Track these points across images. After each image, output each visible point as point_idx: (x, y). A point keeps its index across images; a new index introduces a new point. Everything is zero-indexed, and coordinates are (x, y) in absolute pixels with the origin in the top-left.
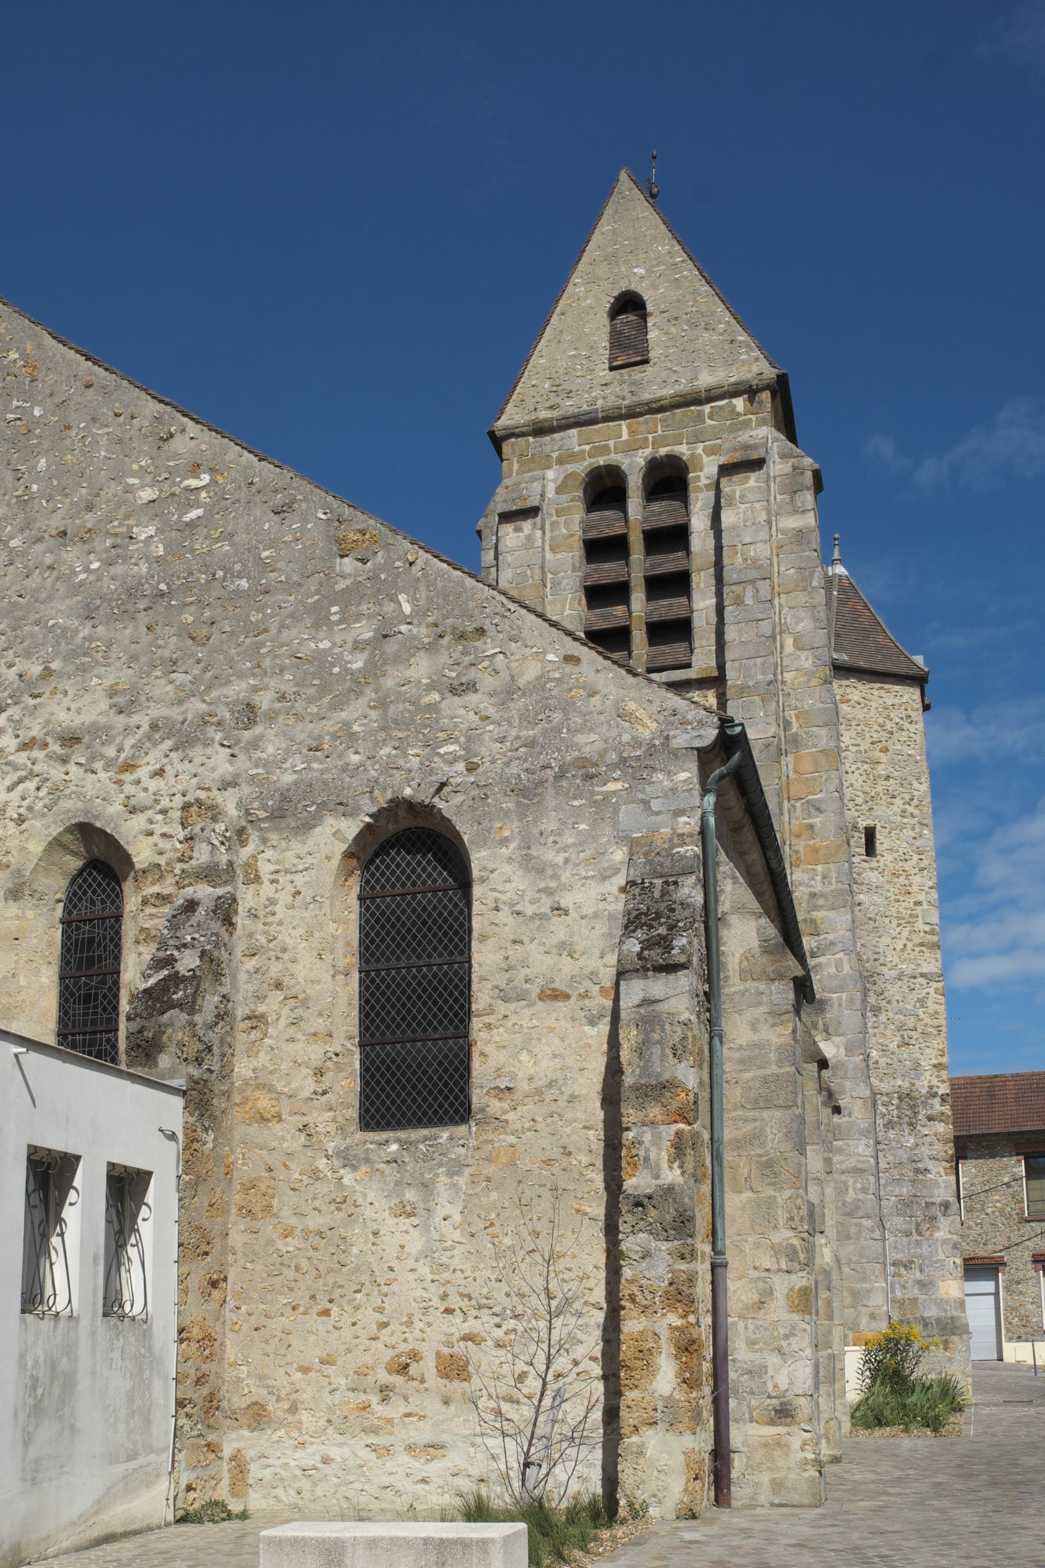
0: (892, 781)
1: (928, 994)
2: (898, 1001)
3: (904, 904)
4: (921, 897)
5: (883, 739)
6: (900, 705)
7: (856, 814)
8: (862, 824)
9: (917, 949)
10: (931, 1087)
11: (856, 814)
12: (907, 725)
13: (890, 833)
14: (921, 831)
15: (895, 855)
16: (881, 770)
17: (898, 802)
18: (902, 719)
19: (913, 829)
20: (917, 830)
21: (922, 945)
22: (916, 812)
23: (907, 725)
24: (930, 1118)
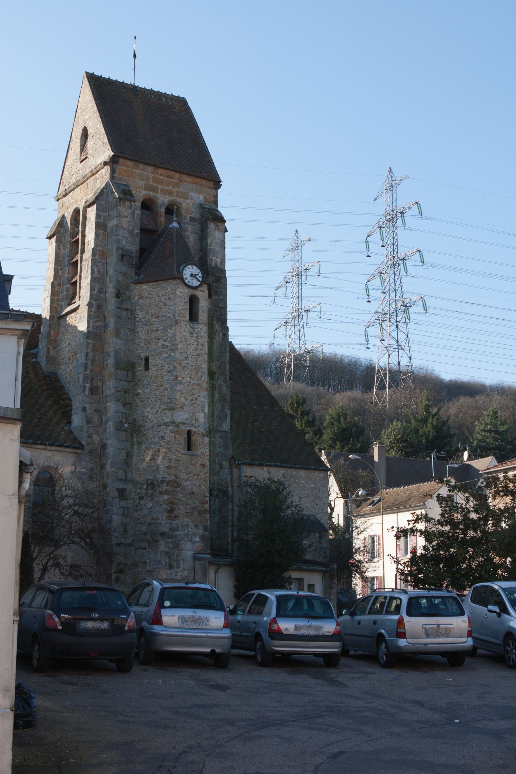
0: (159, 332)
1: (166, 433)
2: (151, 438)
3: (159, 391)
4: (168, 386)
5: (157, 312)
6: (166, 293)
7: (141, 351)
8: (143, 355)
9: (163, 412)
10: (163, 478)
11: (141, 351)
12: (168, 302)
13: (155, 357)
14: (171, 354)
15: (157, 368)
16: (154, 327)
17: (161, 341)
18: (166, 300)
19: (167, 353)
20: (169, 353)
21: (165, 409)
22: (169, 345)
23: (168, 302)
24: (161, 493)
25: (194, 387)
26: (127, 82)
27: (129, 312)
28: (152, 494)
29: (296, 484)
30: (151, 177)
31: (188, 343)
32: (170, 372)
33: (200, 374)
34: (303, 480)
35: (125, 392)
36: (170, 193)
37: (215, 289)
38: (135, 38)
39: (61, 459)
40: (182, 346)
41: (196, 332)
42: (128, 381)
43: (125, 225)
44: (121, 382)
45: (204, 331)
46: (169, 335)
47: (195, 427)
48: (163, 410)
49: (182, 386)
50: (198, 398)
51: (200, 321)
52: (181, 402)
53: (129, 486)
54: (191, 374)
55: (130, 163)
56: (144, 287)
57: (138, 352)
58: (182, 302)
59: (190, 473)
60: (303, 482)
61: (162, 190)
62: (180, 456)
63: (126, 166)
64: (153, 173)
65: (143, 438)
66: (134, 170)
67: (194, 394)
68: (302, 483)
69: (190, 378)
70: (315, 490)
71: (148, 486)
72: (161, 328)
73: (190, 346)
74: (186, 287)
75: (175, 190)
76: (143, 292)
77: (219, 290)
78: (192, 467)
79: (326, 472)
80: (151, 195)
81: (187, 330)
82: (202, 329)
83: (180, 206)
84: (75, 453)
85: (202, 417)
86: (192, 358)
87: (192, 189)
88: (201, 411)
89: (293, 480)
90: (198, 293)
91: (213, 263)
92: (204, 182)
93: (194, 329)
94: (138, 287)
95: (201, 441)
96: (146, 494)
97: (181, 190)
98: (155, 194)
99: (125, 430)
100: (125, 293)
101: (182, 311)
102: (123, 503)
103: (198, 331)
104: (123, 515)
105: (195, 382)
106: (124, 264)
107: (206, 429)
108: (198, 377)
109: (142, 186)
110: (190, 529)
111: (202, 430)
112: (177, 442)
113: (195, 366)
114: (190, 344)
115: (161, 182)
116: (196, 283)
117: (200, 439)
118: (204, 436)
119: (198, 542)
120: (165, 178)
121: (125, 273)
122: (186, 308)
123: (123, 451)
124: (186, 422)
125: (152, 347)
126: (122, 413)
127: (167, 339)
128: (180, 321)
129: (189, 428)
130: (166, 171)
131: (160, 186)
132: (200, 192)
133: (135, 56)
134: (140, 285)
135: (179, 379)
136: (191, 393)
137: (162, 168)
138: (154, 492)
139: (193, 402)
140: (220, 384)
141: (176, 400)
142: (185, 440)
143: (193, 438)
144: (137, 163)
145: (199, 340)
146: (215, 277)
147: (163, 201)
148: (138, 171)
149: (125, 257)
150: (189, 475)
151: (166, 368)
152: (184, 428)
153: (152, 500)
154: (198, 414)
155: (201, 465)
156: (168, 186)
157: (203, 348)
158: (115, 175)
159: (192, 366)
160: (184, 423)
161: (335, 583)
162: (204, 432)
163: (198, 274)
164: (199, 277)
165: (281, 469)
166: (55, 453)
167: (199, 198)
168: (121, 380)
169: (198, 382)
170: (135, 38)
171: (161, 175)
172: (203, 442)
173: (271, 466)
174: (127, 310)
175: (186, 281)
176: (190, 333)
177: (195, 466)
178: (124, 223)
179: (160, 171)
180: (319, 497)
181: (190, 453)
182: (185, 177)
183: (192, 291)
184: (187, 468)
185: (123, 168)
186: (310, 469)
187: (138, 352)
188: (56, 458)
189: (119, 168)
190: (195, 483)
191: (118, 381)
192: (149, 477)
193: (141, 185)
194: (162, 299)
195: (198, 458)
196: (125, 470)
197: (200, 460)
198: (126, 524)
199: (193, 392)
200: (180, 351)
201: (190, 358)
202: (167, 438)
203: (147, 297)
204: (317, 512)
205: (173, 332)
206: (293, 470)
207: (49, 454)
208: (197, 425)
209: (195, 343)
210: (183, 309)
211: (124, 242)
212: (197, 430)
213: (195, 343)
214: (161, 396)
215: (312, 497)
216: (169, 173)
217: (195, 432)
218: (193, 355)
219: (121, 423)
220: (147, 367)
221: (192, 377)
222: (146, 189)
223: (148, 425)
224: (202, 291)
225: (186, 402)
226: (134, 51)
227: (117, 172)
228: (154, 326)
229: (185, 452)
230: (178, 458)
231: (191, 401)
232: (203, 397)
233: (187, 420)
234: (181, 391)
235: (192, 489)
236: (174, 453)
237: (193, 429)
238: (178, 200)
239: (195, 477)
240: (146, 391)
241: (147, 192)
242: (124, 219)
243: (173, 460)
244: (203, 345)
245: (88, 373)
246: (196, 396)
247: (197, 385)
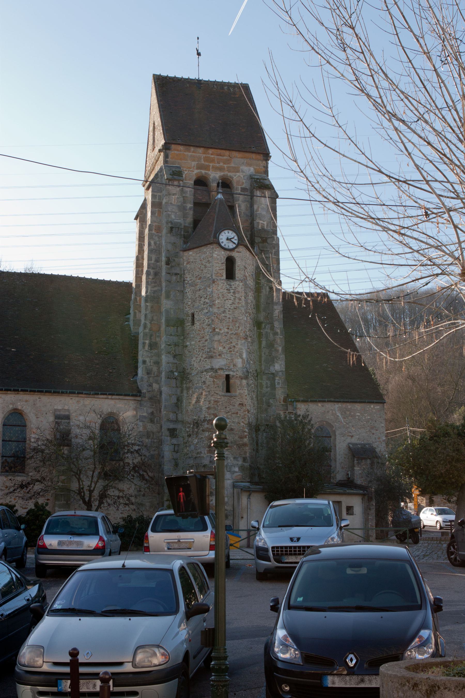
0: (201, 291)
3: (201, 342)
6: (206, 257)
8: (190, 312)
9: (204, 360)
10: (205, 417)
12: (208, 265)
15: (200, 322)
16: (198, 287)
17: (203, 299)
19: (207, 309)
20: (208, 309)
21: (206, 358)
23: (208, 265)
25: (231, 336)
26: (192, 77)
27: (178, 276)
28: (197, 432)
29: (352, 417)
30: (202, 157)
31: (225, 298)
32: (209, 325)
33: (237, 325)
34: (358, 413)
35: (175, 345)
36: (221, 169)
37: (262, 249)
38: (198, 38)
39: (123, 406)
40: (219, 302)
41: (233, 288)
42: (177, 336)
43: (174, 202)
44: (172, 337)
45: (240, 287)
46: (208, 293)
47: (233, 371)
48: (204, 359)
49: (220, 337)
50: (236, 346)
51: (237, 278)
52: (219, 350)
53: (179, 426)
55: (181, 148)
56: (191, 253)
57: (186, 310)
58: (219, 263)
59: (229, 412)
60: (359, 414)
61: (213, 167)
62: (219, 397)
63: (178, 150)
64: (204, 153)
65: (190, 385)
66: (186, 153)
67: (231, 343)
68: (358, 416)
69: (228, 328)
70: (370, 421)
71: (194, 425)
72: (203, 287)
73: (227, 301)
74: (223, 250)
75: (225, 166)
76: (190, 257)
77: (265, 249)
78: (231, 407)
79: (382, 404)
80: (203, 173)
81: (224, 287)
82: (239, 285)
83: (231, 179)
84: (135, 400)
85: (239, 362)
86: (229, 311)
87: (243, 163)
88: (239, 357)
89: (348, 413)
90: (234, 254)
91: (260, 227)
92: (254, 156)
93: (230, 285)
94: (186, 254)
95: (239, 383)
96: (193, 432)
97: (232, 165)
98: (207, 172)
99: (175, 378)
100: (174, 260)
101: (219, 271)
102: (174, 441)
103: (235, 287)
104: (174, 451)
105: (233, 332)
106: (174, 236)
107: (244, 373)
108: (236, 327)
109: (194, 166)
110: (229, 461)
111: (240, 374)
112: (216, 385)
113: (233, 318)
114: (228, 299)
115: (213, 161)
116: (231, 246)
117: (238, 382)
118: (242, 379)
119: (236, 472)
120: (216, 156)
121: (174, 243)
122: (222, 268)
123: (173, 396)
124: (224, 368)
125: (196, 305)
126: (172, 363)
127: (207, 296)
128: (217, 280)
130: (216, 150)
131: (211, 164)
132: (250, 165)
133: (199, 54)
134: (187, 252)
135: (217, 330)
136: (228, 342)
137: (211, 148)
138: (199, 429)
139: (232, 350)
140: (266, 332)
141: (214, 349)
142: (223, 383)
143: (232, 381)
144: (188, 147)
145: (237, 295)
146: (261, 238)
148: (190, 154)
149: (174, 229)
150: (229, 414)
151: (207, 322)
152: (222, 373)
153: (197, 437)
154: (236, 360)
155: (240, 404)
156: (219, 163)
157: (240, 302)
158: (168, 160)
159: (229, 318)
160: (222, 369)
161: (372, 505)
162: (242, 375)
163: (234, 238)
164: (235, 240)
165: (336, 404)
166: (117, 401)
167: (250, 170)
168: (171, 335)
169: (236, 332)
170: (198, 38)
171: (212, 154)
172: (241, 384)
173: (324, 401)
174: (176, 274)
175: (223, 245)
176: (227, 290)
177: (234, 406)
178: (173, 200)
179: (210, 151)
180: (375, 427)
181: (228, 394)
182: (234, 154)
183: (228, 252)
184: (226, 407)
185: (176, 152)
186: (365, 402)
187: (186, 310)
188: (118, 406)
189: (171, 153)
190: (234, 421)
191: (168, 336)
192: (195, 418)
193: (193, 165)
194: (203, 262)
195: (237, 398)
196: (175, 412)
197: (238, 400)
198: (177, 459)
199: (231, 341)
200: (217, 306)
201: (227, 312)
202: (208, 383)
203: (192, 262)
204: (374, 440)
205: (210, 290)
206: (348, 404)
207: (112, 402)
208: (235, 370)
209: (232, 298)
210: (220, 270)
211: (173, 217)
212: (235, 374)
214: (203, 346)
215: (369, 428)
216: (219, 151)
217: (233, 376)
218: (230, 309)
219: (172, 372)
220: (193, 323)
222: (197, 169)
223: (194, 373)
224: (238, 252)
225: (224, 350)
226: (197, 51)
227: (170, 156)
228: (198, 286)
229: (223, 394)
230: (217, 399)
231: (229, 349)
232: (241, 345)
233: (225, 365)
234: (219, 341)
235: (231, 426)
236: (213, 395)
237: (231, 373)
238: (229, 174)
239: (234, 415)
240: (193, 343)
241: (199, 171)
242: (174, 197)
243: (212, 402)
244: (240, 299)
245: (148, 331)
246: (234, 344)
247: (235, 335)
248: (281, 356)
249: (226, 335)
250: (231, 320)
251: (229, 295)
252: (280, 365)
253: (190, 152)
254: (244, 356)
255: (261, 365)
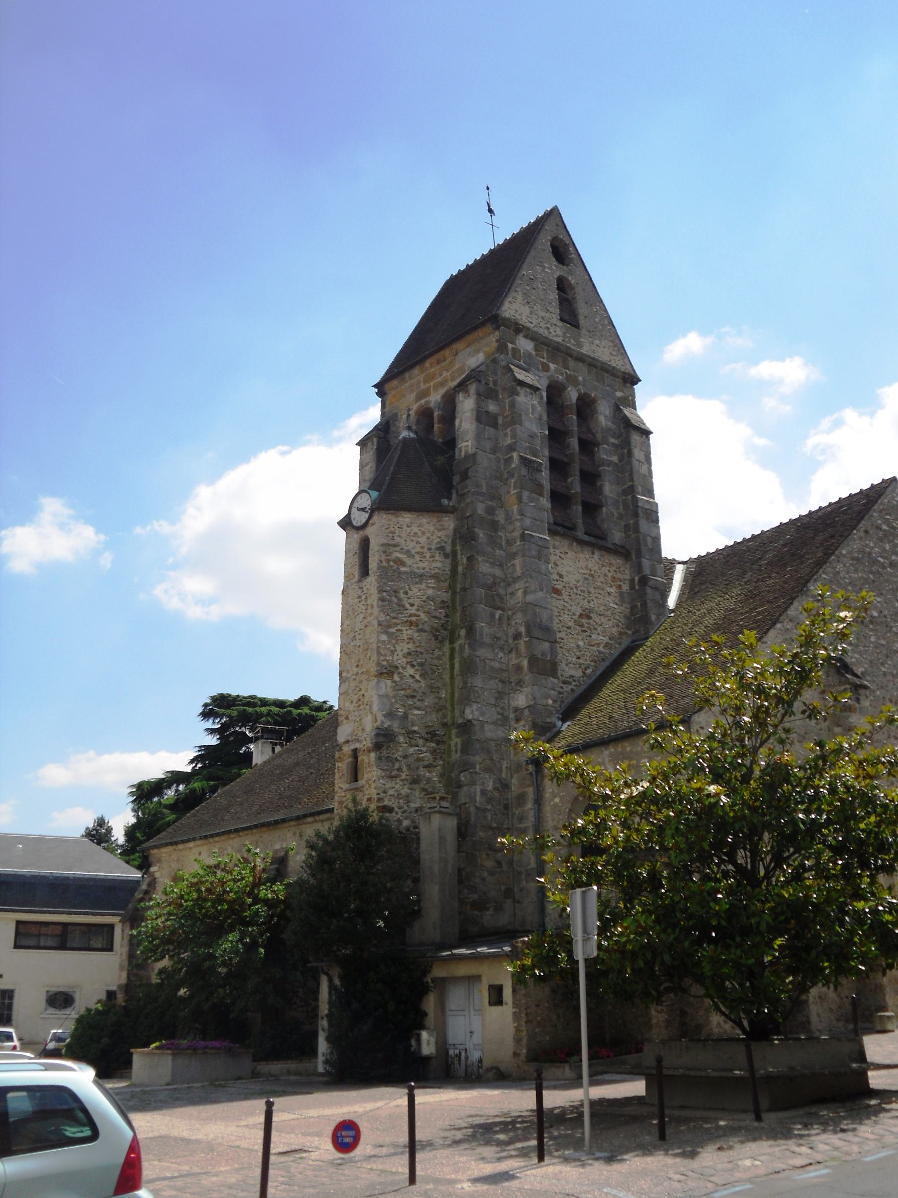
31: (356, 614)
38: (488, 188)
54: (359, 661)
55: (395, 383)
64: (422, 372)
67: (360, 690)
75: (448, 374)
77: (466, 490)
87: (470, 354)
91: (463, 454)
92: (480, 333)
97: (457, 366)
107: (372, 739)
111: (368, 744)
112: (341, 774)
118: (369, 751)
124: (350, 738)
129: (353, 747)
131: (432, 384)
132: (477, 351)
133: (491, 211)
136: (357, 689)
147: (436, 401)
148: (407, 385)
170: (488, 188)
171: (431, 367)
179: (427, 364)
181: (354, 785)
183: (361, 532)
189: (389, 397)
201: (358, 637)
209: (364, 608)
212: (362, 746)
213: (364, 608)
221: (360, 664)
226: (489, 206)
227: (387, 406)
233: (352, 734)
237: (357, 745)
241: (418, 404)
248: (527, 678)
249: (355, 680)
250: (361, 649)
251: (360, 605)
252: (527, 696)
253: (407, 382)
254: (375, 708)
255: (453, 711)
